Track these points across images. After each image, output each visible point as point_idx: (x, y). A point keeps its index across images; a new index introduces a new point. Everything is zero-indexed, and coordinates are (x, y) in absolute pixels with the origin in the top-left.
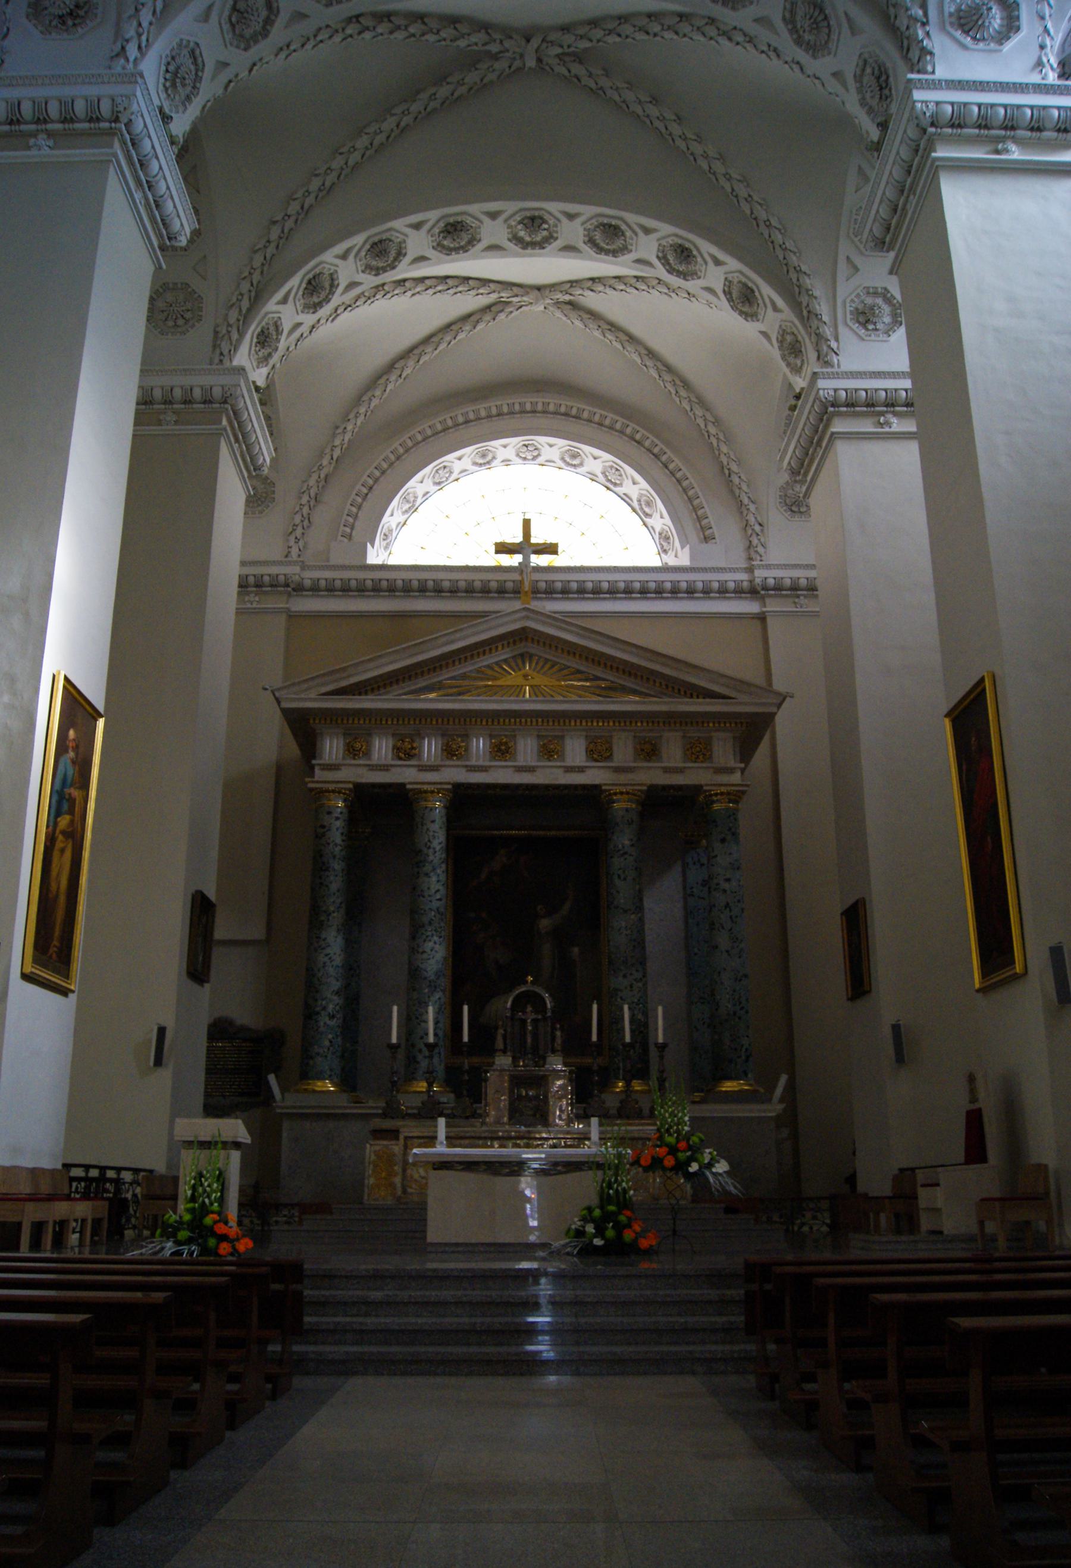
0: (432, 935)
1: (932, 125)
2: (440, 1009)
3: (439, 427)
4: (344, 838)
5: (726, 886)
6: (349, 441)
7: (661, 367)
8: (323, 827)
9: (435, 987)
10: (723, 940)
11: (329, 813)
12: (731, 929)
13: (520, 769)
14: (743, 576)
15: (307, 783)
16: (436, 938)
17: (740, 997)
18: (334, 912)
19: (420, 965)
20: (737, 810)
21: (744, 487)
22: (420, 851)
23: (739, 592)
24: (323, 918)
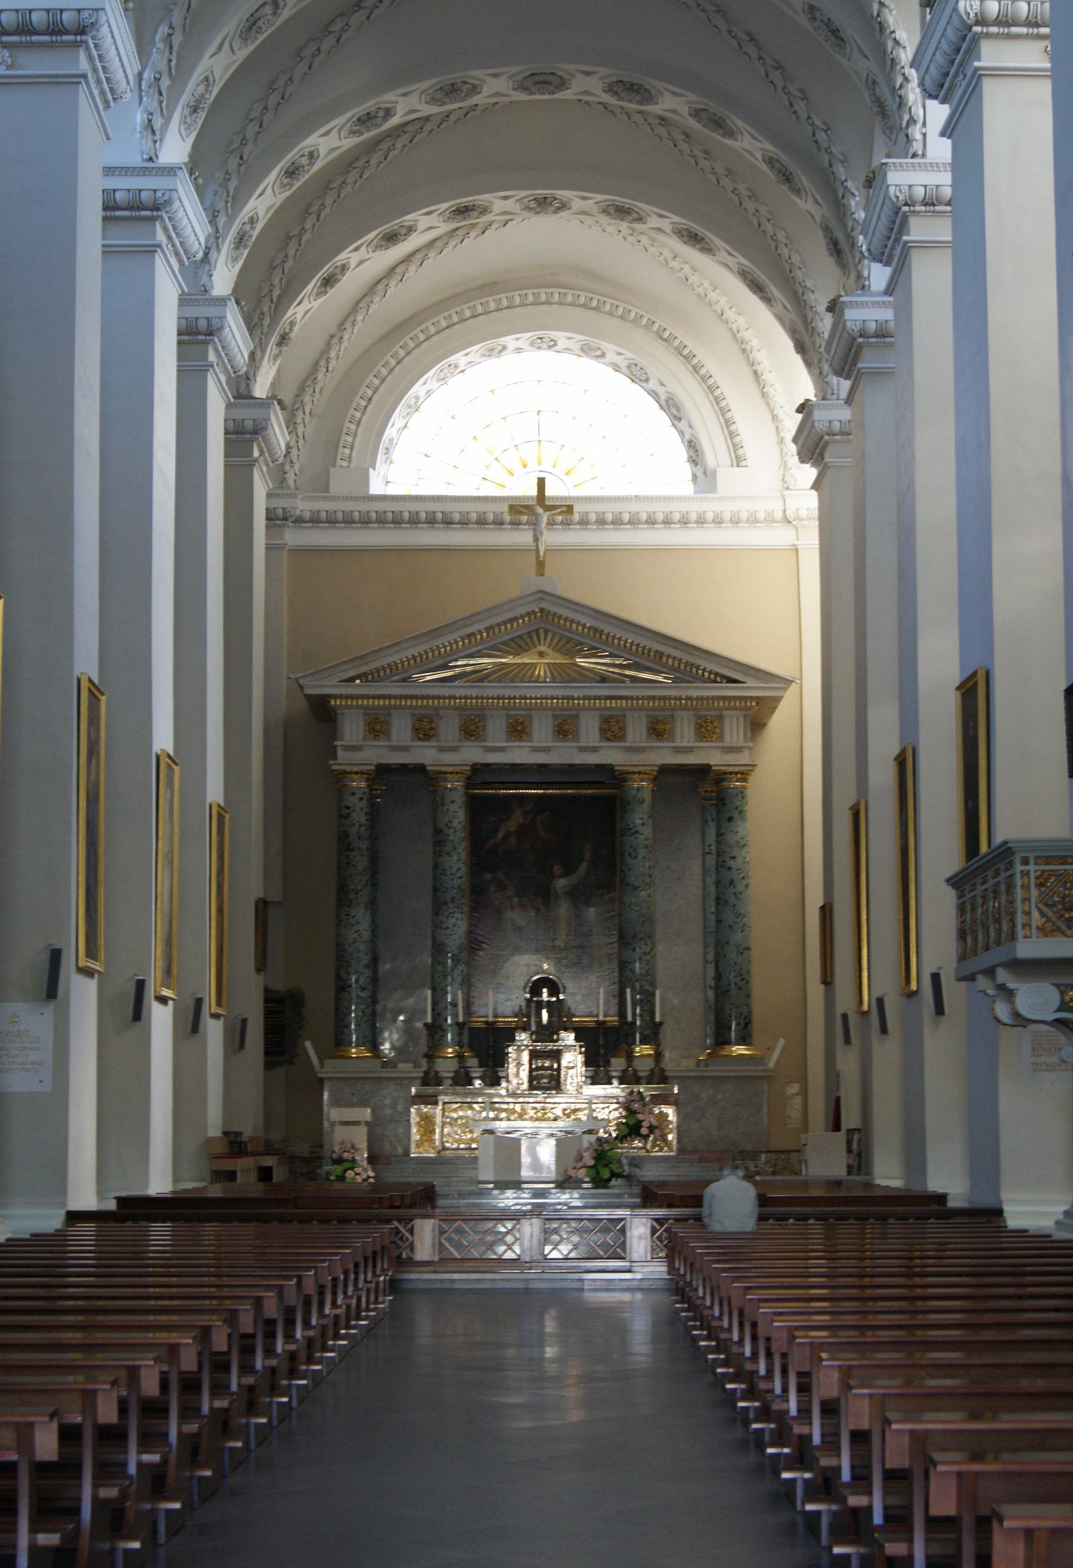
0: (454, 912)
1: (861, 336)
2: (463, 980)
3: (444, 324)
4: (368, 817)
6: (346, 348)
8: (348, 808)
9: (459, 961)
11: (353, 794)
12: (734, 906)
13: (535, 750)
15: (330, 765)
16: (458, 915)
17: (741, 969)
18: (361, 890)
19: (445, 941)
20: (745, 788)
22: (441, 831)
24: (352, 896)
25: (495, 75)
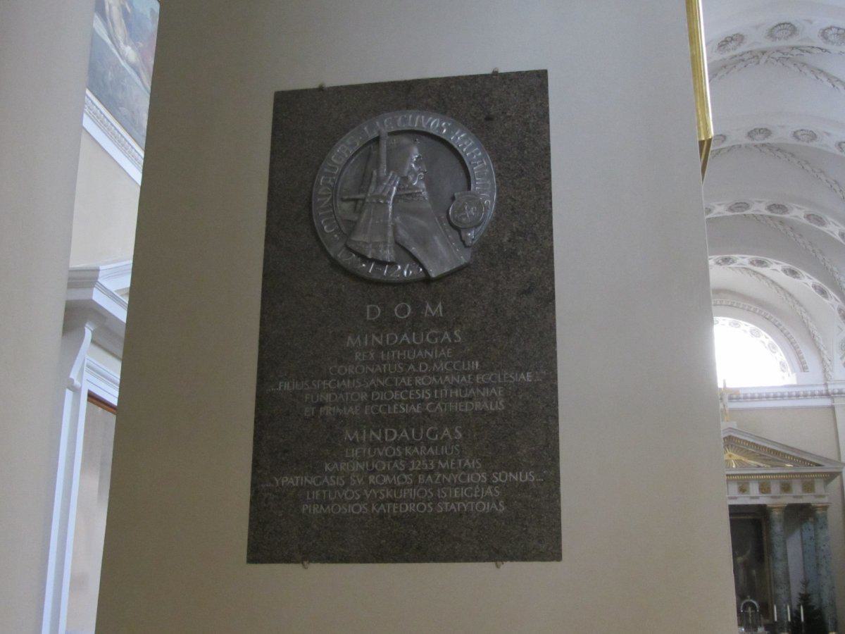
5: (822, 548)
7: (779, 289)
10: (823, 572)
14: (823, 389)
21: (821, 342)
23: (821, 395)
25: (720, 205)
